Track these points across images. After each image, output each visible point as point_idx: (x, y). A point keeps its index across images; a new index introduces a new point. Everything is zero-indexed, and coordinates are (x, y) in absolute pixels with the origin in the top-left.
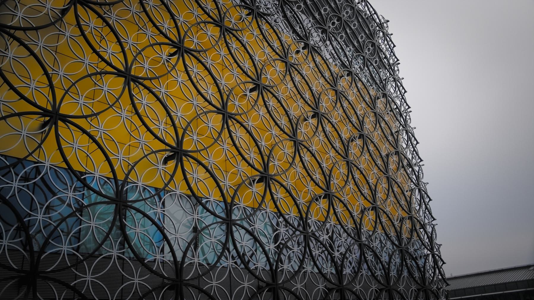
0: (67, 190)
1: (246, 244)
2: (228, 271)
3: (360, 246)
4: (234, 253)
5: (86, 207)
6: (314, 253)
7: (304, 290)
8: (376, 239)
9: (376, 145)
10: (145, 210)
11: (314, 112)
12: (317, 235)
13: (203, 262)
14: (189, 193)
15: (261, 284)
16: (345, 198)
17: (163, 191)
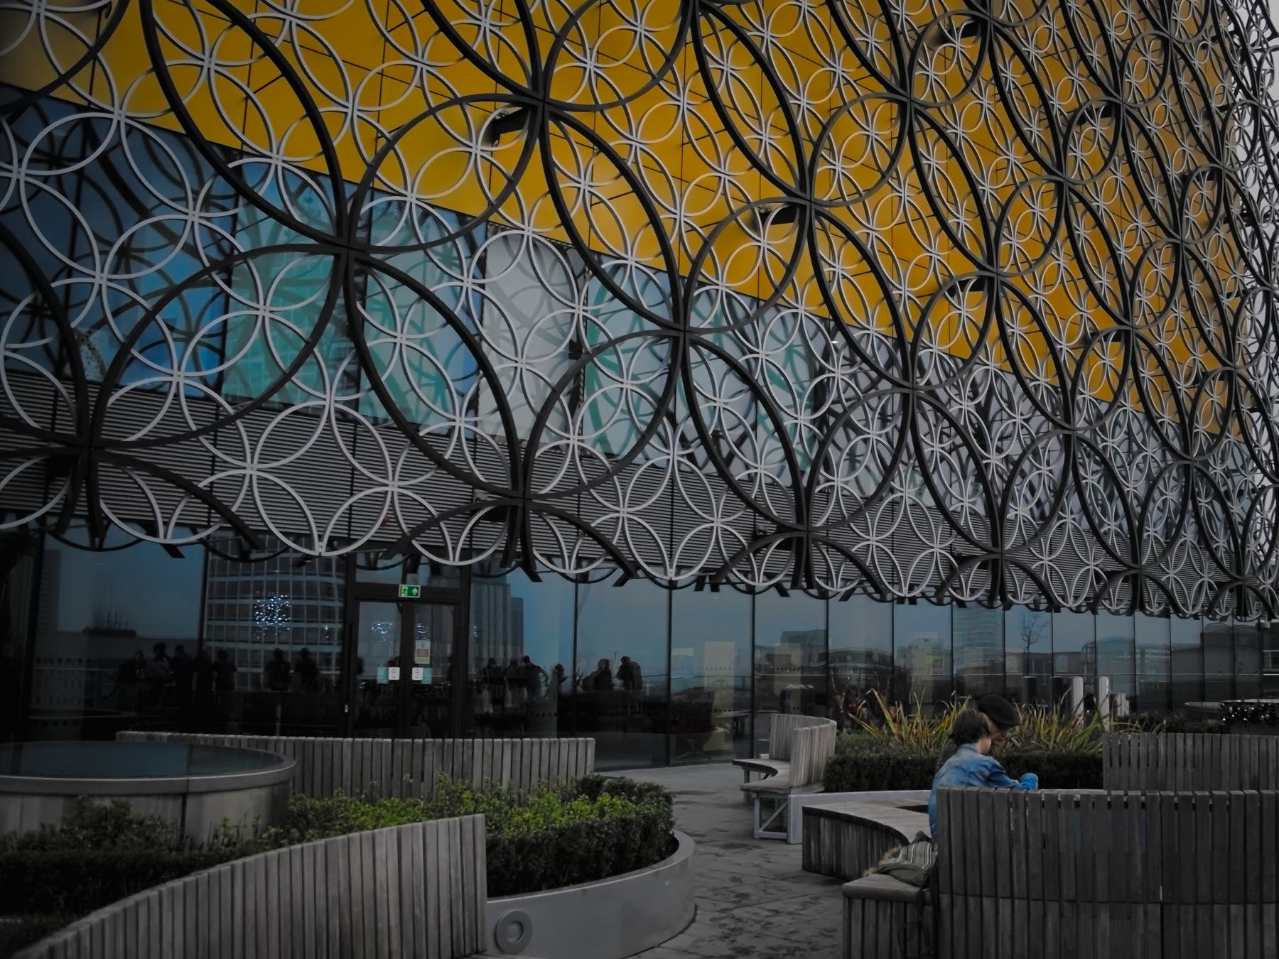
0: (184, 202)
1: (726, 404)
2: (667, 480)
3: (1067, 443)
4: (688, 427)
5: (245, 257)
6: (927, 451)
7: (886, 553)
8: (1118, 428)
9: (1156, 141)
10: (424, 279)
11: (973, 17)
12: (944, 398)
13: (594, 447)
14: (564, 237)
15: (762, 525)
16: (1040, 296)
17: (483, 226)
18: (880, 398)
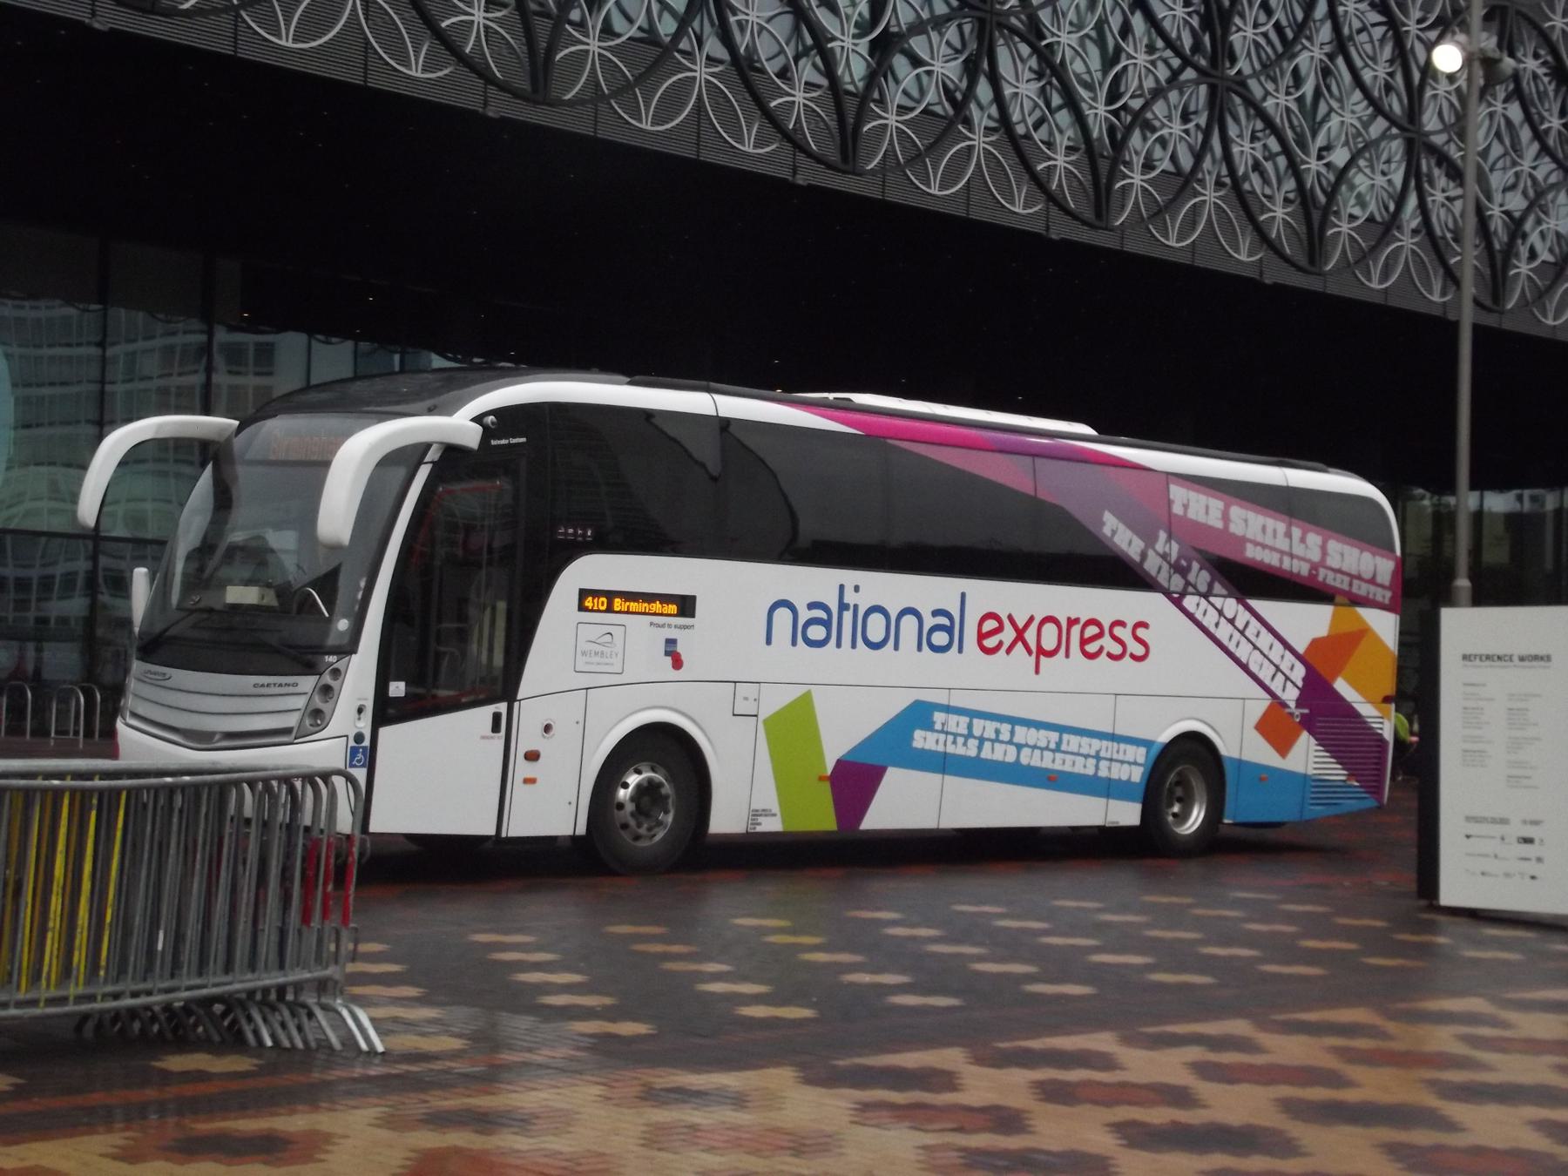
18: (1182, 93)
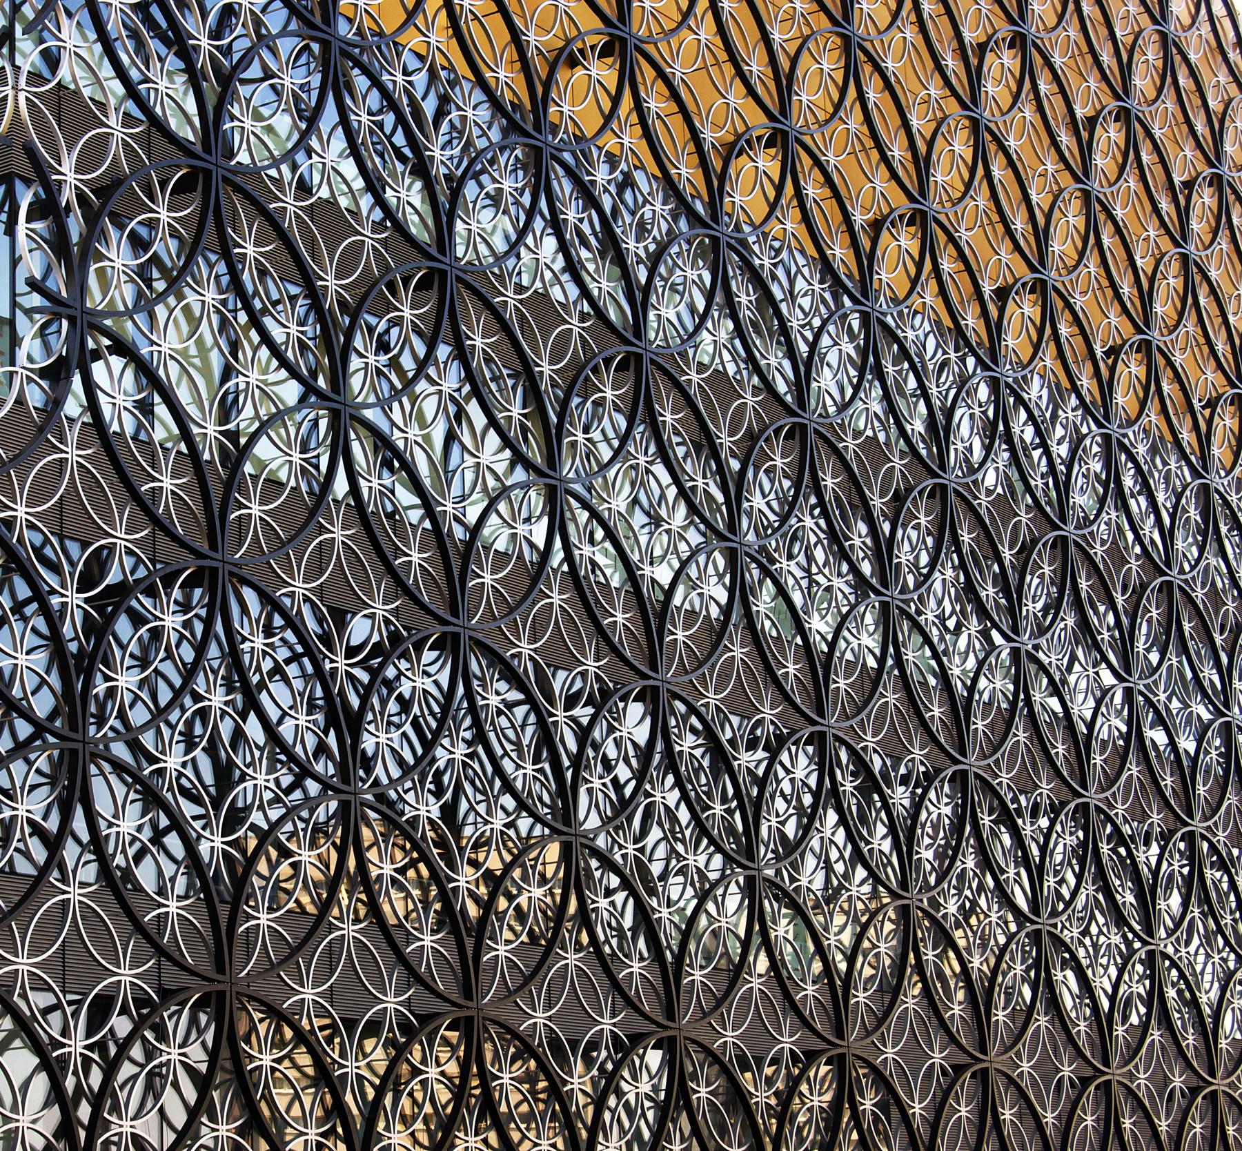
11: (610, 35)
